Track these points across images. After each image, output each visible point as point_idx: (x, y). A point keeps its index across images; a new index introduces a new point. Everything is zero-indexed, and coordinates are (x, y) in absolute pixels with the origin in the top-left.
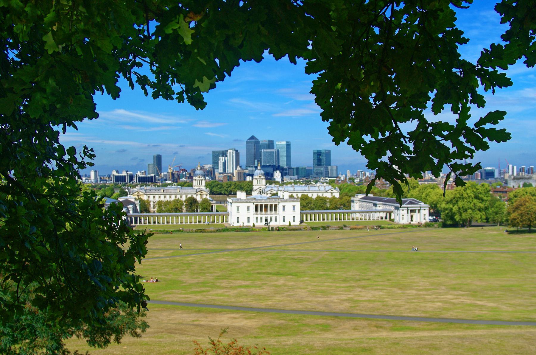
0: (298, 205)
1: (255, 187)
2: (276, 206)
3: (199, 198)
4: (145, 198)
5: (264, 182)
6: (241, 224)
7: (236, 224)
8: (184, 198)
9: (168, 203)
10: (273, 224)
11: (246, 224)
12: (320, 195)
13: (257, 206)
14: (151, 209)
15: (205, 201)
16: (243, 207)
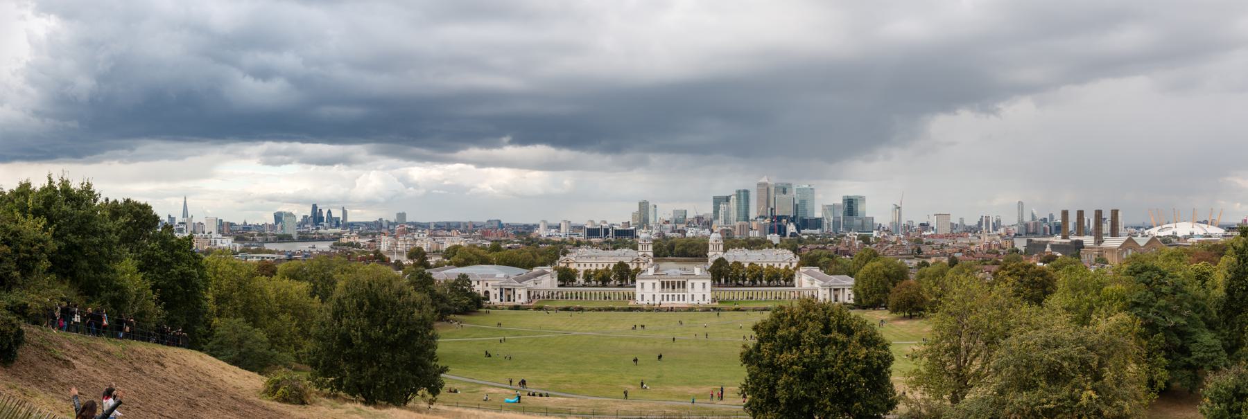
0: (709, 283)
1: (710, 254)
2: (684, 283)
3: (633, 267)
4: (573, 266)
5: (721, 248)
6: (645, 302)
7: (640, 302)
8: (611, 268)
9: (597, 271)
10: (680, 303)
11: (651, 302)
12: (777, 265)
13: (663, 283)
14: (580, 280)
15: (638, 270)
16: (648, 284)
